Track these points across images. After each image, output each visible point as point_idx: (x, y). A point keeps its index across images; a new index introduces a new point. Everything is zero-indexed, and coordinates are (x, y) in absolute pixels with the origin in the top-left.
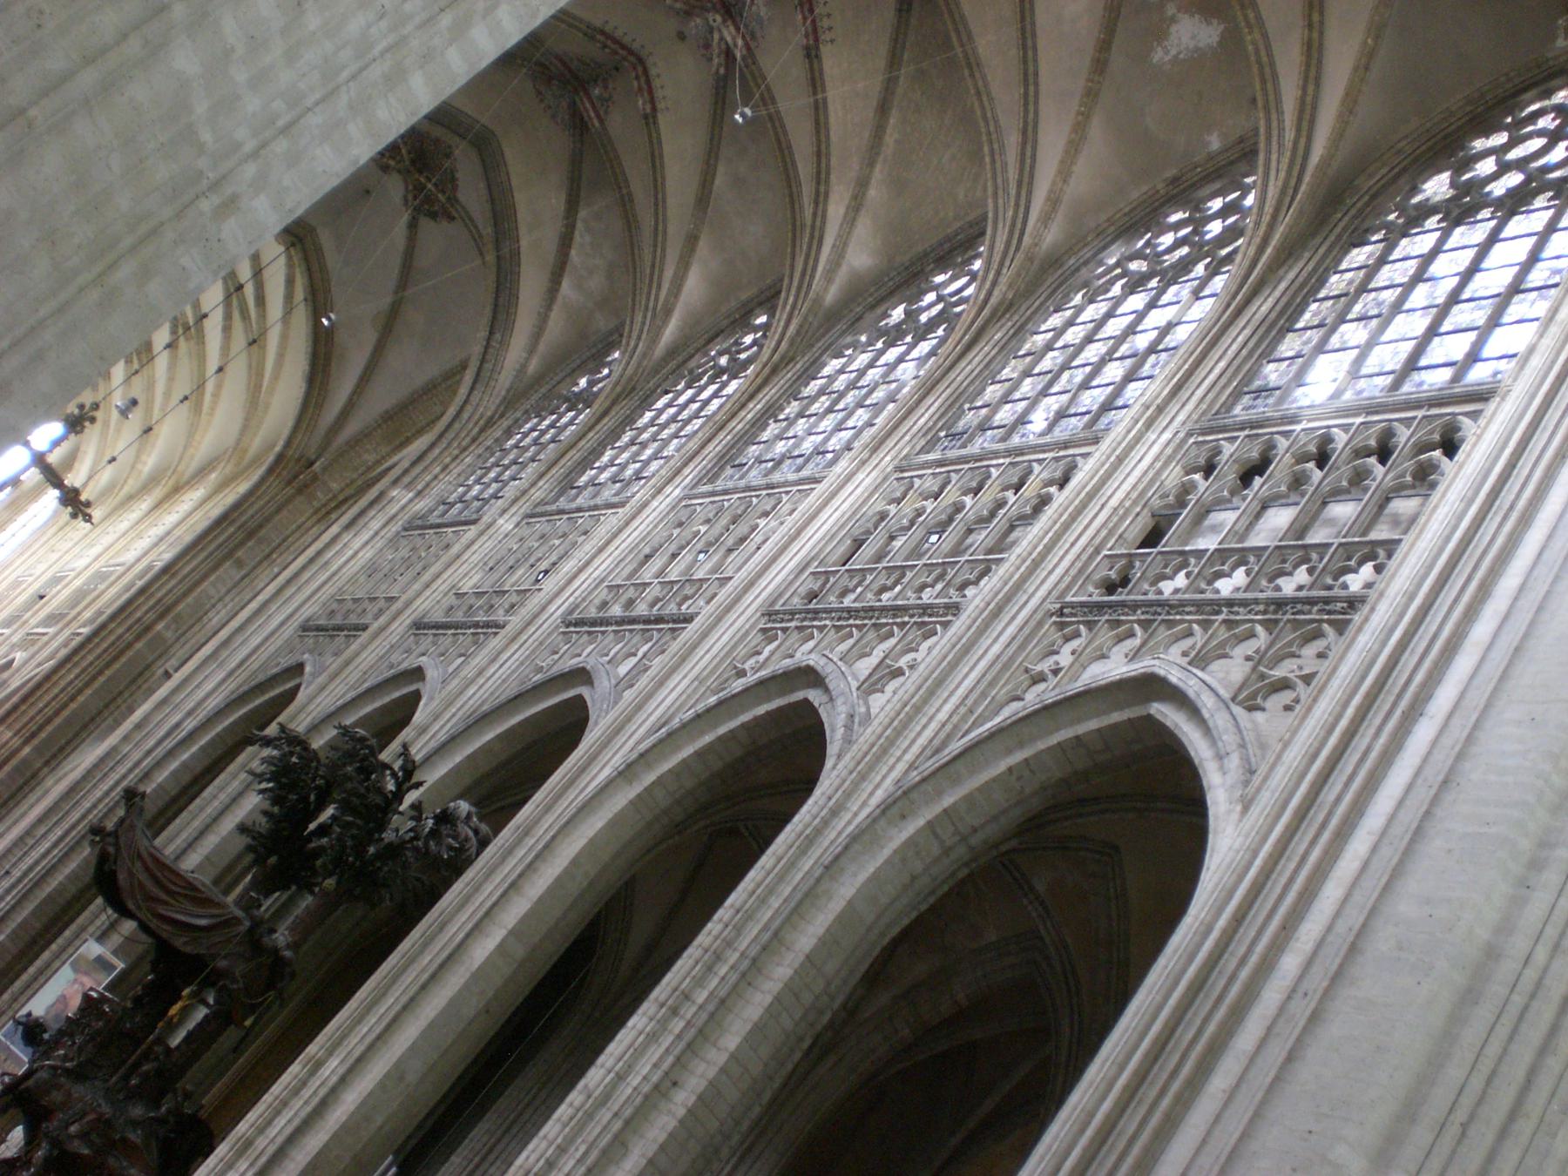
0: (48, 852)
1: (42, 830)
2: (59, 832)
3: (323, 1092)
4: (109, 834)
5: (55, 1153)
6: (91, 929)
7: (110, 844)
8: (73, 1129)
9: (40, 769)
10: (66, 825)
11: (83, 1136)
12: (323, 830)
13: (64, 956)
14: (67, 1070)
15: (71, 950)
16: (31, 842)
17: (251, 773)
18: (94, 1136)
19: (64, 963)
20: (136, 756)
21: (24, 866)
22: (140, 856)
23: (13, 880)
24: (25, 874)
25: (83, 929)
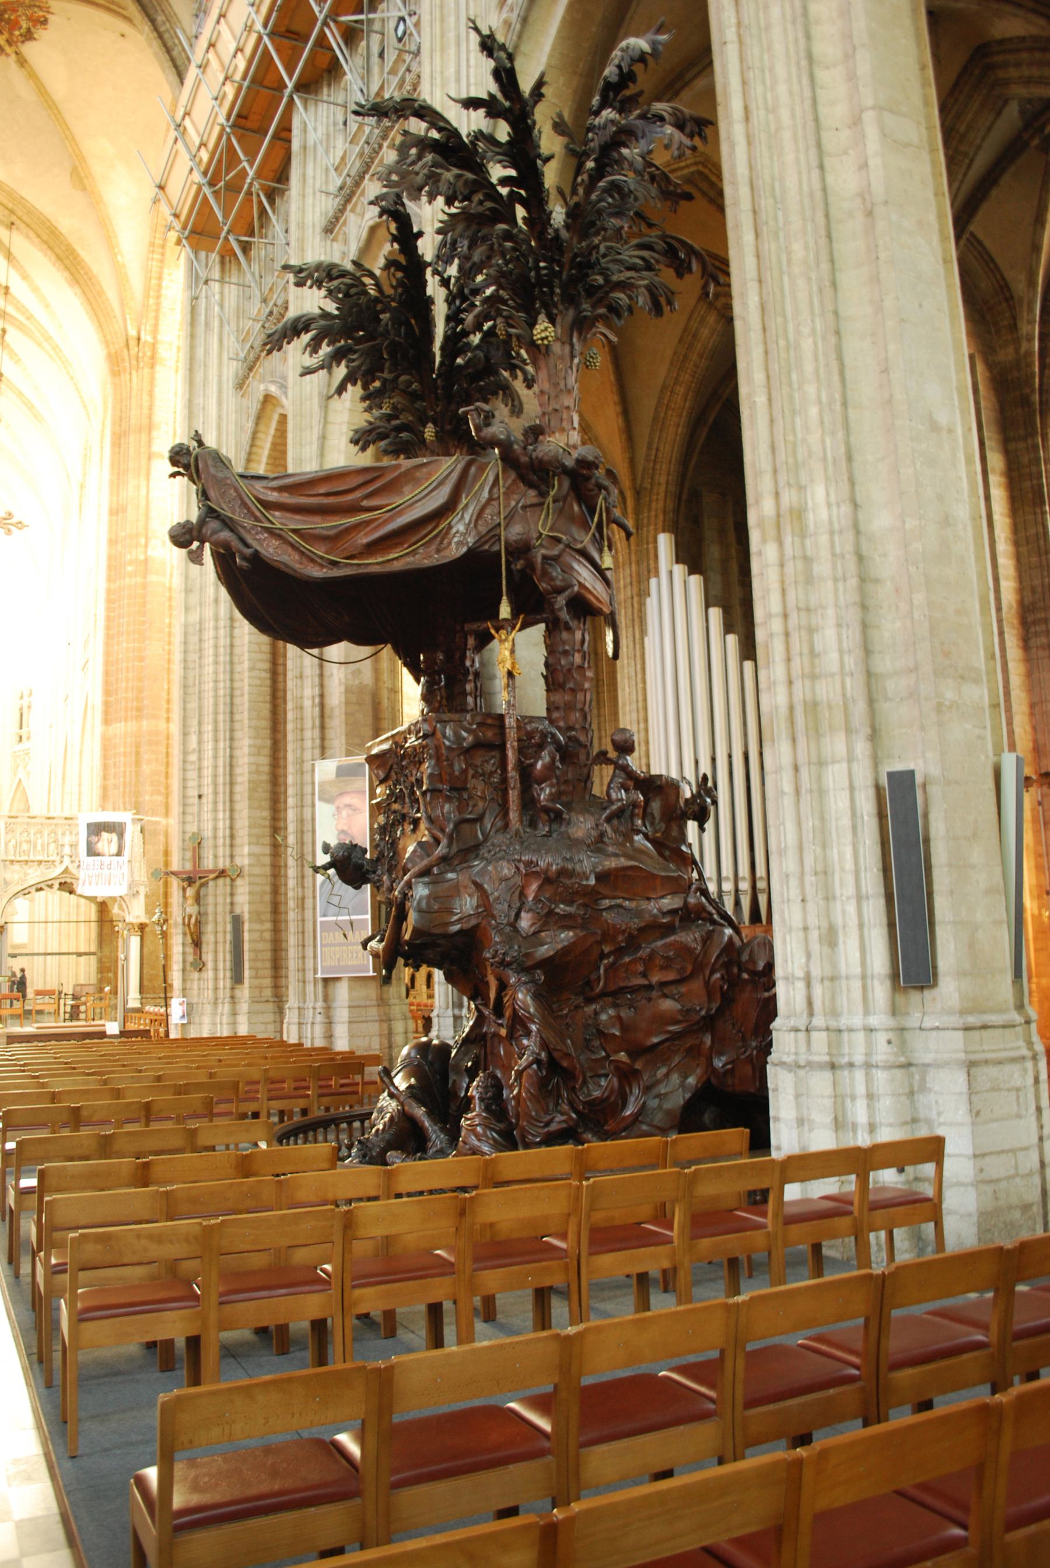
0: (216, 749)
1: (193, 739)
2: (208, 728)
3: (845, 544)
4: (202, 522)
5: (540, 976)
6: (308, 755)
7: (214, 533)
8: (525, 922)
9: (168, 728)
10: (208, 718)
11: (548, 919)
12: (454, 343)
13: (308, 800)
14: (444, 859)
15: (308, 789)
16: (193, 757)
17: (308, 372)
18: (562, 908)
19: (313, 805)
20: (209, 612)
21: (207, 780)
22: (268, 505)
23: (211, 797)
24: (215, 784)
25: (301, 762)
